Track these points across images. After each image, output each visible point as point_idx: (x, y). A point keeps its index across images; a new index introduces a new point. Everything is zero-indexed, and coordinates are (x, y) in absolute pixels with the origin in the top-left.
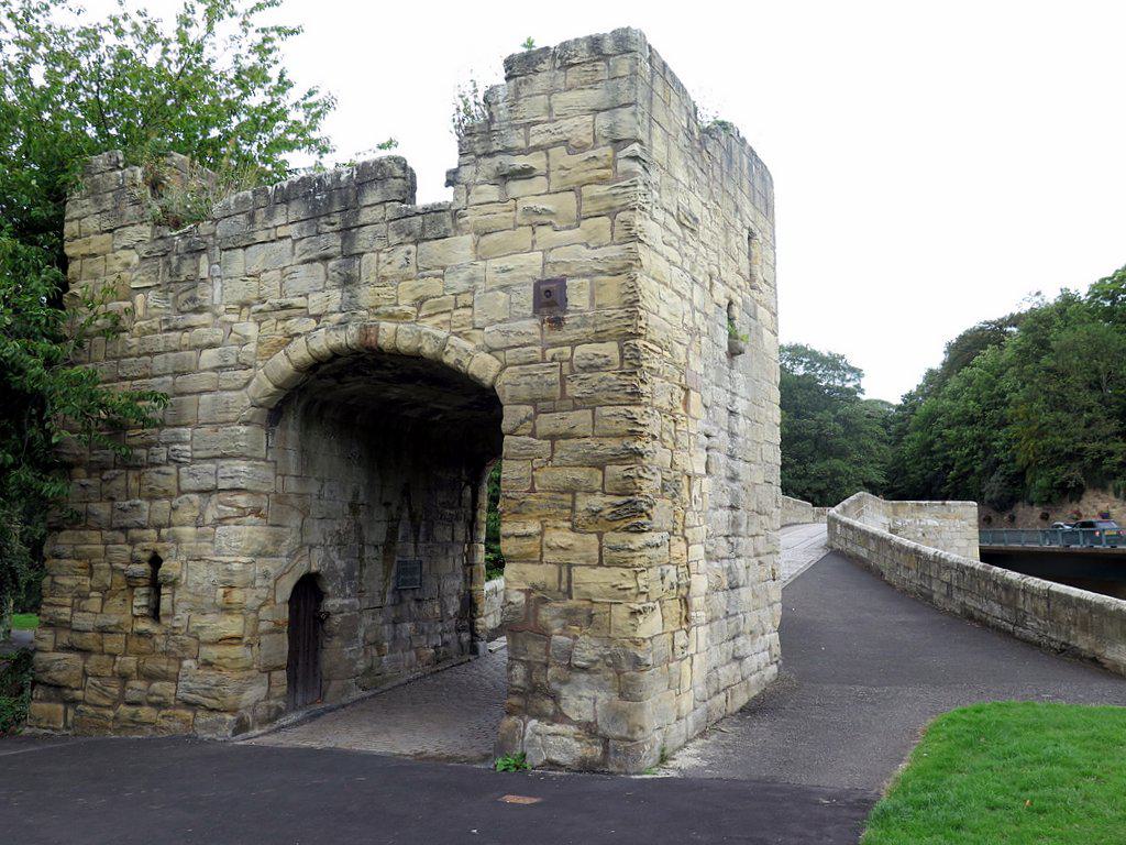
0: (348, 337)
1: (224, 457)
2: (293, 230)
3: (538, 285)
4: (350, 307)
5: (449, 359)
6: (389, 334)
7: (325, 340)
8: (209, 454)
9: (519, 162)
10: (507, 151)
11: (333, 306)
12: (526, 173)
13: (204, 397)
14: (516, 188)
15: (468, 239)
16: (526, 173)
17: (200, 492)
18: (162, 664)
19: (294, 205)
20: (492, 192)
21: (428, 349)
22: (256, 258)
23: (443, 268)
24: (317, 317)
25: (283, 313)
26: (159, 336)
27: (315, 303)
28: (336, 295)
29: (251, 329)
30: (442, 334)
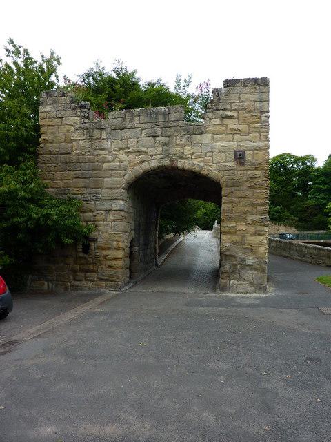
0: (166, 162)
1: (115, 199)
2: (144, 126)
3: (235, 152)
4: (166, 155)
5: (204, 173)
6: (181, 164)
7: (154, 164)
8: (108, 198)
9: (229, 113)
10: (225, 110)
11: (159, 153)
12: (231, 117)
13: (106, 179)
14: (227, 121)
15: (209, 135)
16: (231, 117)
17: (105, 211)
18: (91, 267)
19: (142, 117)
20: (217, 122)
21: (197, 169)
22: (127, 134)
23: (201, 144)
24: (152, 156)
25: (138, 154)
26: (86, 157)
27: (151, 151)
28: (160, 150)
29: (124, 157)
30: (202, 164)
